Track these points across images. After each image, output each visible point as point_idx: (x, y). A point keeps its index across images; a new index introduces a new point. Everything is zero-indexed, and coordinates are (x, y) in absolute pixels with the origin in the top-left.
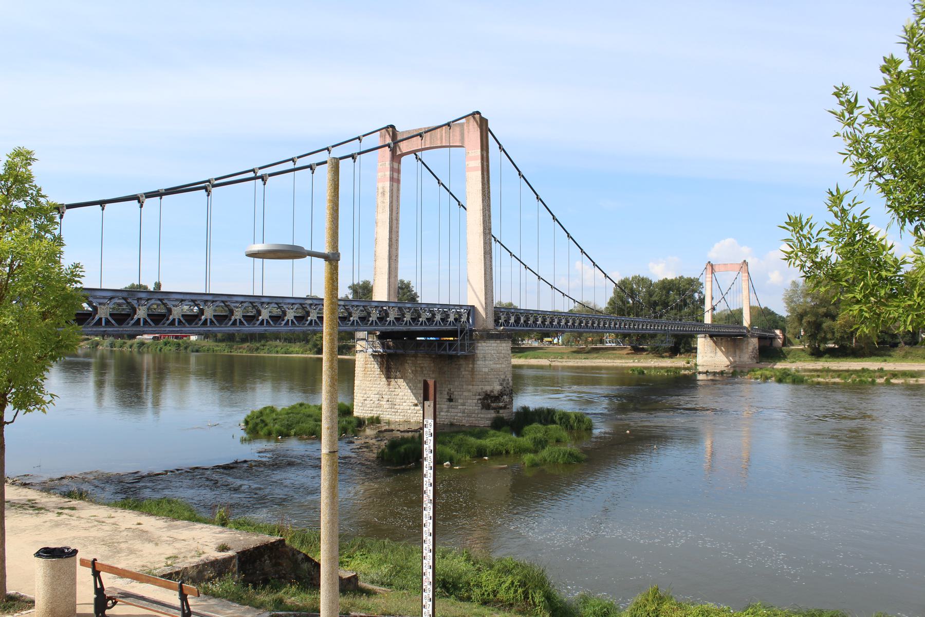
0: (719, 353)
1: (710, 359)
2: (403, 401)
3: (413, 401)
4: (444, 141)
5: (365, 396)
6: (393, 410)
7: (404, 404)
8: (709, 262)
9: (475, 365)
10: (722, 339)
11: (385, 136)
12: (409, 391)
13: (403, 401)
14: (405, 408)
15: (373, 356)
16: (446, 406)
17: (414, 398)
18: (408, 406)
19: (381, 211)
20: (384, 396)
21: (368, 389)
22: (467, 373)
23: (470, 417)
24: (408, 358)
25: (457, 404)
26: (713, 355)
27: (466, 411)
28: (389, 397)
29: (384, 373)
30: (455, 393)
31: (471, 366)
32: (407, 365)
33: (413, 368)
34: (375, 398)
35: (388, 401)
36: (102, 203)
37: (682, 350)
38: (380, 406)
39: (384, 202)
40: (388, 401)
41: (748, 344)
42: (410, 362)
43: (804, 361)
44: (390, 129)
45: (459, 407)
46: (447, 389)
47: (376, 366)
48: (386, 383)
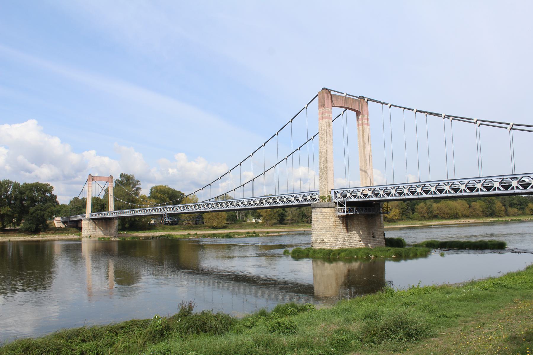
0: (98, 229)
1: (92, 233)
2: (355, 240)
3: (359, 239)
4: (352, 106)
6: (350, 246)
7: (355, 242)
8: (90, 175)
10: (99, 221)
11: (328, 94)
12: (357, 234)
13: (355, 240)
14: (356, 243)
15: (339, 217)
16: (372, 240)
17: (359, 238)
20: (345, 239)
21: (338, 235)
22: (378, 223)
23: (381, 244)
24: (354, 217)
25: (376, 238)
26: (94, 230)
28: (348, 239)
30: (375, 233)
32: (355, 220)
33: (358, 222)
34: (341, 240)
35: (348, 241)
36: (404, 108)
37: (42, 230)
38: (344, 244)
39: (329, 131)
40: (348, 241)
41: (114, 223)
43: (161, 232)
44: (325, 90)
45: (377, 240)
46: (372, 232)
47: (341, 222)
48: (346, 231)
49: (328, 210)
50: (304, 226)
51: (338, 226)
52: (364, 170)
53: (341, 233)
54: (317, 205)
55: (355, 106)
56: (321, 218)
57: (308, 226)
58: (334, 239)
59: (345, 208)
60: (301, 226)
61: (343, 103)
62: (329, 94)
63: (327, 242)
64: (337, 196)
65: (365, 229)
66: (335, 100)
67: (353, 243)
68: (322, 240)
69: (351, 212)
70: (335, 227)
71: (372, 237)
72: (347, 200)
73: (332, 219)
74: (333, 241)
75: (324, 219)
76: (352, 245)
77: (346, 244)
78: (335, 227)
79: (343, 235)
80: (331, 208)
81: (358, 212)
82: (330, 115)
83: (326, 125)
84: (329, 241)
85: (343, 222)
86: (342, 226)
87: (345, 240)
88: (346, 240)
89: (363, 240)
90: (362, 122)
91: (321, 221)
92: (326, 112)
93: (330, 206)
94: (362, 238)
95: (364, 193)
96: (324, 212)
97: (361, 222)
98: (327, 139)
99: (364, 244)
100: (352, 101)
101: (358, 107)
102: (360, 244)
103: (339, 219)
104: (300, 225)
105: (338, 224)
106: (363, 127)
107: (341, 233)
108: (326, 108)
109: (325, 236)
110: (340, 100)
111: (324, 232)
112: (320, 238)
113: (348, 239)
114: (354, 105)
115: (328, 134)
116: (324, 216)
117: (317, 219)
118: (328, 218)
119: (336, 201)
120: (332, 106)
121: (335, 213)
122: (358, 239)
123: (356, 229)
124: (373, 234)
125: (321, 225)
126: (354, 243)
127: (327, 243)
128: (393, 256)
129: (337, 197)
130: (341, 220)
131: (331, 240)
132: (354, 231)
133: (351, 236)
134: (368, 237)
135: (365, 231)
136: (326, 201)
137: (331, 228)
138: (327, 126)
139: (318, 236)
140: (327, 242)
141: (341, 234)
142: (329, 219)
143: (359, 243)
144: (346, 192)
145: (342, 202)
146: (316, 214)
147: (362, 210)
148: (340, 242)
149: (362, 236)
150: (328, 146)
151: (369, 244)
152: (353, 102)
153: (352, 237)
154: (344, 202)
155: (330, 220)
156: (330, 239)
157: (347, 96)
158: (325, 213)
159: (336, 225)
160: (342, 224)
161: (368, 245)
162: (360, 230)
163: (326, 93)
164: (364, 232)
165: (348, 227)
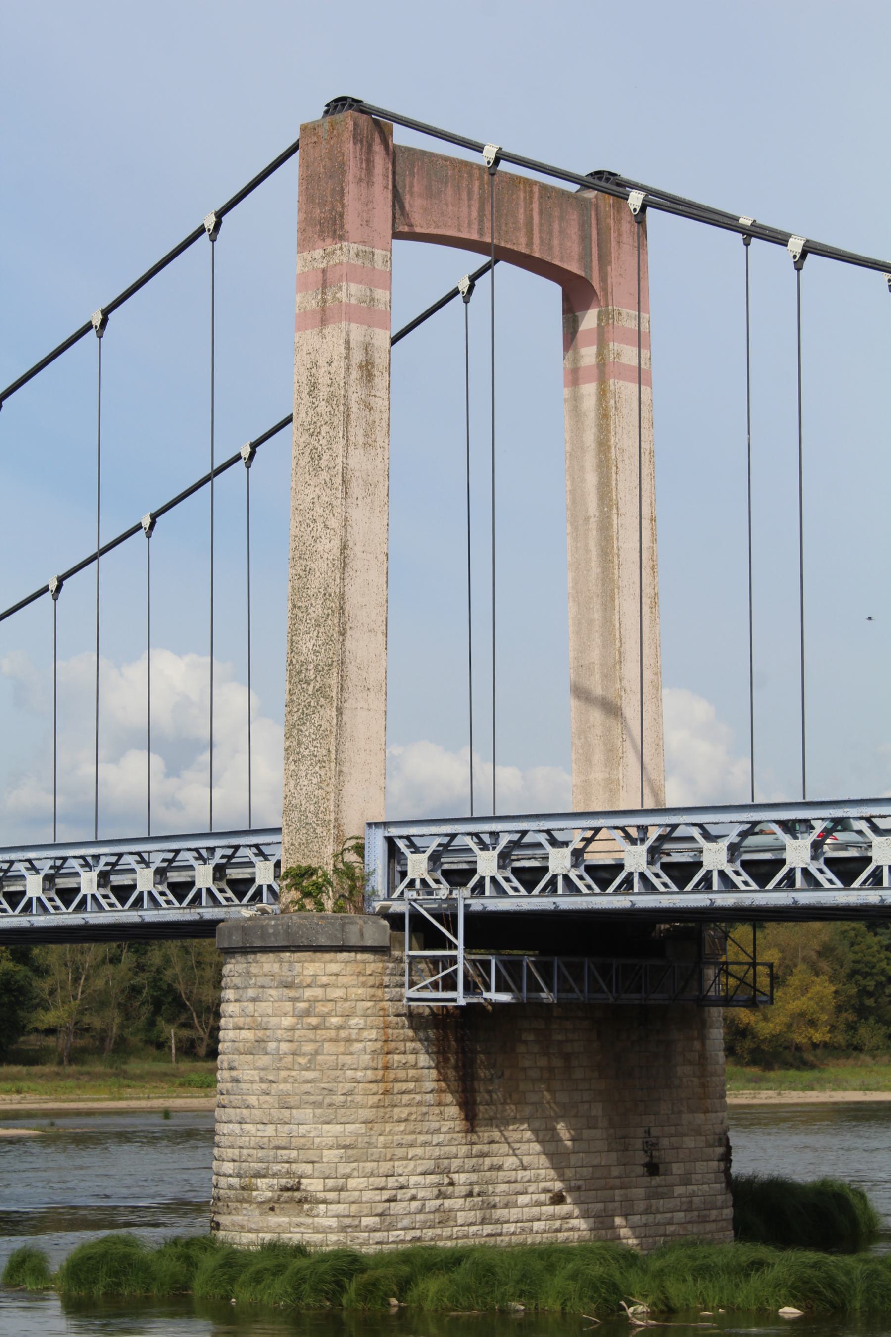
2: (518, 1187)
3: (548, 1185)
4: (536, 240)
5: (392, 1182)
6: (488, 1229)
7: (522, 1199)
9: (708, 1042)
11: (370, 146)
12: (537, 1147)
13: (518, 1187)
14: (529, 1212)
15: (415, 1019)
16: (641, 1192)
17: (552, 1173)
18: (539, 1204)
19: (361, 440)
20: (455, 1176)
21: (400, 1152)
22: (688, 1069)
23: (703, 1220)
27: (696, 1200)
28: (474, 1177)
29: (454, 1085)
30: (665, 1142)
31: (697, 1045)
33: (543, 1062)
35: (470, 1195)
38: (445, 1218)
39: (369, 407)
40: (470, 1195)
42: (531, 1037)
44: (347, 117)
45: (679, 1190)
46: (641, 1132)
47: (424, 1059)
48: (459, 1125)
49: (334, 967)
50: (164, 1076)
51: (404, 1086)
52: (599, 691)
53: (422, 1138)
54: (264, 936)
55: (556, 242)
56: (287, 1021)
57: (194, 1077)
58: (372, 1175)
59: (461, 960)
60: (140, 1077)
61: (475, 214)
62: (378, 148)
63: (324, 1202)
64: (404, 874)
65: (597, 1110)
66: (416, 189)
67: (507, 1206)
68: (291, 1182)
69: (498, 990)
70: (386, 1092)
71: (640, 1170)
72: (477, 905)
73: (366, 1034)
74: (368, 1196)
75: (310, 1034)
76: (497, 1222)
77: (461, 1217)
78: (386, 1092)
79: (436, 1152)
80: (360, 956)
81: (551, 990)
82: (380, 294)
83: (348, 368)
84: (341, 1190)
85: (440, 1054)
86: (430, 1086)
87: (452, 1184)
88: (462, 1190)
89: (578, 1188)
90: (601, 354)
91: (284, 1047)
92: (352, 275)
93: (354, 941)
94: (569, 1173)
95: (597, 855)
96: (309, 980)
97: (567, 1057)
98: (353, 462)
99: (585, 1215)
100: (535, 206)
101: (574, 247)
102: (553, 1217)
103: (411, 1033)
104: (135, 1066)
105: (402, 1074)
106: (603, 394)
107: (428, 1138)
108: (355, 247)
109: (312, 1155)
110: (450, 191)
111: (303, 1129)
112: (276, 1167)
113: (474, 1177)
114: (550, 232)
115: (357, 433)
116: (307, 1013)
117: (260, 1034)
118: (339, 1028)
119: (397, 907)
120: (397, 235)
121: (389, 993)
122: (542, 1185)
123: (527, 1110)
124: (650, 1146)
125: (283, 1073)
126: (514, 1213)
127: (322, 1207)
128: (789, 1312)
129: (407, 881)
130: (427, 1039)
131: (352, 1183)
132: (515, 1120)
133: (496, 1161)
134: (615, 1171)
135: (592, 1125)
136: (329, 904)
137: (359, 1098)
138: (355, 374)
139: (261, 1153)
140: (321, 1196)
141: (425, 1144)
142: (343, 1034)
143: (550, 1209)
144: (470, 842)
145: (437, 917)
146: (251, 993)
147: (578, 979)
148: (414, 1198)
149: (573, 1160)
150: (356, 514)
151: (618, 1221)
152: (541, 212)
153: (500, 1168)
154: (455, 916)
155: (349, 1040)
156: (348, 1176)
157: (504, 166)
158: (318, 992)
159: (391, 1074)
160: (434, 1073)
161: (613, 1227)
162: (557, 1118)
163: (355, 137)
164: (586, 1133)
165: (473, 1091)
